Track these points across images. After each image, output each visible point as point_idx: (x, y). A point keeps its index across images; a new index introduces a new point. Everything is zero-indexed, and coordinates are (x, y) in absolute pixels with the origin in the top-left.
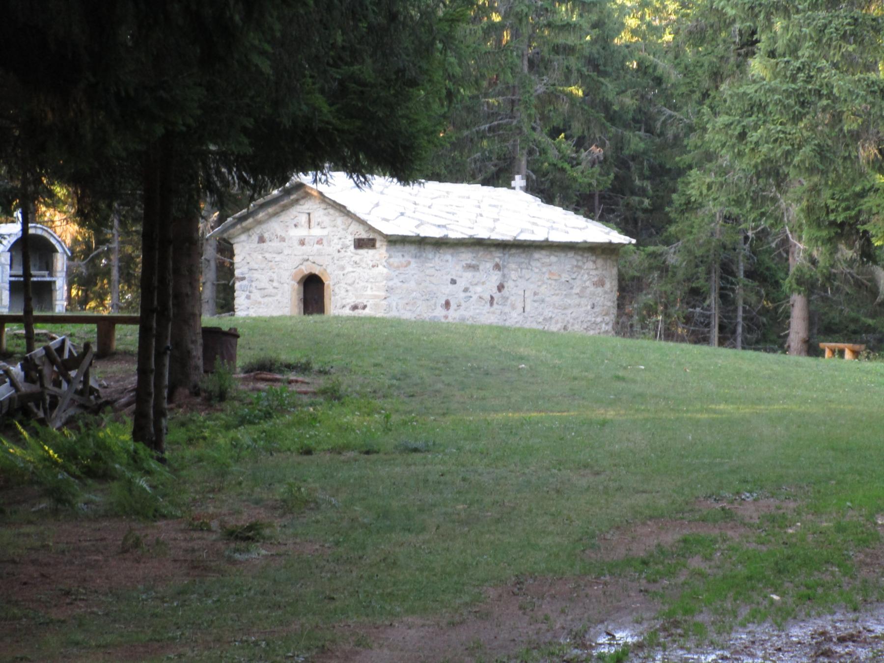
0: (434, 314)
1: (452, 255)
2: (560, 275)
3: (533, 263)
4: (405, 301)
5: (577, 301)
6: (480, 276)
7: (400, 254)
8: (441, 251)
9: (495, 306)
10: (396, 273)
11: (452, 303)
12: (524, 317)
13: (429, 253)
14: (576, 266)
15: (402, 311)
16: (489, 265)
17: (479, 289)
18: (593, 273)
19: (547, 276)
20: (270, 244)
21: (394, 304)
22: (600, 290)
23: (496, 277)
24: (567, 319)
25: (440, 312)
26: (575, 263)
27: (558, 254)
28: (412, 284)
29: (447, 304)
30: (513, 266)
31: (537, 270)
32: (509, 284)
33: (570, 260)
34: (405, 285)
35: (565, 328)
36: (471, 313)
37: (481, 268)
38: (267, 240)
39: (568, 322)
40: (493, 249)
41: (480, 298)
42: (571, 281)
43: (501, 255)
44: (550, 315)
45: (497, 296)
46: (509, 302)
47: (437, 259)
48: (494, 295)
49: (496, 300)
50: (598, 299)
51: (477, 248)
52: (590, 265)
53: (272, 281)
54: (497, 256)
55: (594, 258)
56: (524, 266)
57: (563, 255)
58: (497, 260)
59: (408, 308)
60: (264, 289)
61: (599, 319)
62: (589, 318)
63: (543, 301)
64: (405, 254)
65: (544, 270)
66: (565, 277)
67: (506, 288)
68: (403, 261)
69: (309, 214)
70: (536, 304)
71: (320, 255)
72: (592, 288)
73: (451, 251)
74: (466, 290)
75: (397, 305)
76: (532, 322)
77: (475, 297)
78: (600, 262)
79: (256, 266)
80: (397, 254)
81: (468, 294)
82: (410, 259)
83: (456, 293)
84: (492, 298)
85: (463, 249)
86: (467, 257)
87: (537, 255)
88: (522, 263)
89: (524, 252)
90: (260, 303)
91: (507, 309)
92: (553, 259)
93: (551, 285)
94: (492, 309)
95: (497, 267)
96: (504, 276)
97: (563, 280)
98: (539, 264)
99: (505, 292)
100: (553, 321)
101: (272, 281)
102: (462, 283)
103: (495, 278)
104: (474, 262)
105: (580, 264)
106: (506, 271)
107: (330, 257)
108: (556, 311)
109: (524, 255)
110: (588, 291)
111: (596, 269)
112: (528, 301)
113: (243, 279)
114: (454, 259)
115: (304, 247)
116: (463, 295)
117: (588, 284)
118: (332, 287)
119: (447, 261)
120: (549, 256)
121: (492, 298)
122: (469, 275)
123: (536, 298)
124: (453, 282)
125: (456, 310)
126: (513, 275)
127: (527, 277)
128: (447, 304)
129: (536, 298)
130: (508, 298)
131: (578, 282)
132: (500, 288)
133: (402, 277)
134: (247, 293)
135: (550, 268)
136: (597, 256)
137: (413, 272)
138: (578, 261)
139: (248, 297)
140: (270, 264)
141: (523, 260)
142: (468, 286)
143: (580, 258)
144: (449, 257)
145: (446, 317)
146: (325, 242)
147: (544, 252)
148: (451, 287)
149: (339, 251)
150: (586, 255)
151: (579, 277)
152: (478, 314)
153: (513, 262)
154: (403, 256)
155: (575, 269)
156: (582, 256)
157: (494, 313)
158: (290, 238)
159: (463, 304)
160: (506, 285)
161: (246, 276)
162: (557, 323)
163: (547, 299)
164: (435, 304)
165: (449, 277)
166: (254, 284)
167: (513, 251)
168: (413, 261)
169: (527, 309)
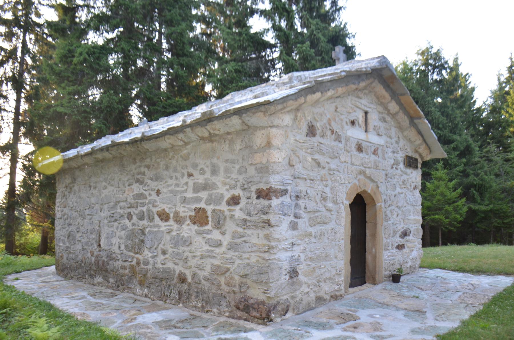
20: (321, 140)
38: (318, 132)
53: (325, 199)
60: (315, 212)
69: (366, 113)
71: (377, 167)
79: (304, 173)
90: (310, 235)
101: (325, 199)
107: (384, 172)
113: (285, 192)
115: (361, 155)
118: (384, 210)
134: (292, 218)
139: (294, 226)
140: (323, 172)
146: (379, 152)
149: (392, 168)
158: (347, 139)
161: (289, 188)
166: (301, 202)
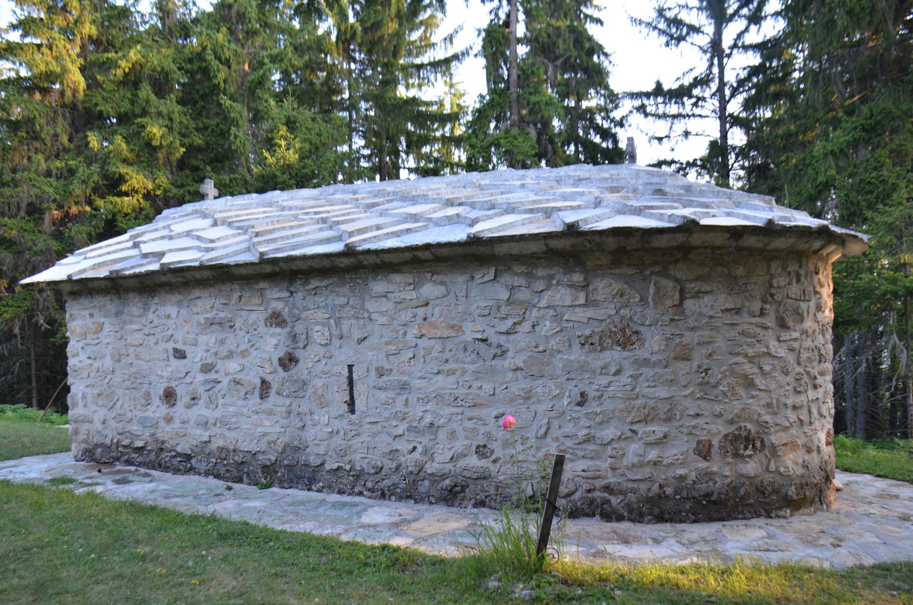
0: (147, 414)
1: (179, 304)
2: (458, 329)
3: (371, 306)
4: (96, 391)
5: (519, 386)
6: (236, 340)
7: (86, 313)
8: (156, 300)
9: (273, 397)
10: (81, 344)
11: (181, 391)
12: (351, 423)
13: (134, 305)
14: (509, 302)
15: (94, 408)
16: (258, 316)
17: (233, 366)
18: (582, 314)
19: (414, 331)
21: (80, 396)
22: (614, 356)
23: (274, 341)
24: (482, 430)
25: (157, 410)
26: (504, 295)
27: (447, 279)
28: (108, 362)
29: (169, 396)
30: (321, 315)
31: (383, 320)
32: (307, 359)
33: (484, 292)
34: (97, 364)
35: (482, 451)
36: (217, 414)
37: (239, 323)
39: (488, 435)
40: (263, 285)
41: (237, 383)
42: (494, 339)
43: (286, 294)
44: (428, 419)
45: (277, 378)
46: (310, 391)
47: (151, 316)
48: (269, 378)
49: (275, 387)
50: (604, 380)
51: (226, 287)
52: (561, 296)
54: (276, 298)
55: (578, 278)
56: (348, 312)
57: (461, 279)
58: (279, 306)
59: (101, 403)
61: (609, 433)
62: (569, 428)
63: (404, 387)
64: (96, 312)
65: (405, 316)
66: (470, 331)
67: (300, 364)
68: (89, 321)
70: (382, 395)
72: (577, 354)
73: (177, 297)
74: (207, 368)
75: (84, 397)
76: (375, 435)
77: (225, 381)
78: (604, 287)
80: (82, 312)
81: (212, 376)
82: (102, 320)
83: (188, 375)
84: (263, 382)
85: (197, 292)
86: (207, 305)
87: (378, 286)
88: (342, 306)
89: (344, 284)
91: (304, 408)
92: (430, 290)
93: (428, 351)
94: (268, 404)
95: (276, 319)
96: (294, 337)
97: (469, 336)
98: (387, 306)
99: (301, 370)
100: (442, 435)
102: (196, 356)
103: (273, 343)
104: (222, 315)
105: (523, 295)
106: (299, 328)
108: (448, 410)
109: (346, 290)
110: (559, 362)
111: (588, 304)
112: (358, 388)
114: (184, 312)
116: (201, 377)
117: (553, 343)
119: (168, 317)
120: (416, 286)
121: (263, 382)
122: (209, 339)
123: (381, 382)
124: (180, 355)
125: (188, 407)
126: (319, 335)
127: (357, 335)
128: (169, 396)
129: (381, 382)
130: (304, 383)
131: (521, 338)
132: (288, 361)
133: (89, 349)
135: (421, 312)
136: (589, 274)
137: (108, 340)
138: (512, 289)
141: (343, 300)
142: (209, 361)
143: (519, 281)
144: (172, 310)
145: (169, 420)
147: (397, 278)
148: (175, 363)
150: (540, 272)
151: (526, 326)
152: (236, 415)
153: (316, 308)
154: (91, 315)
155: (504, 310)
156: (529, 275)
157: (270, 413)
159: (204, 397)
160: (299, 354)
162: (453, 435)
163: (416, 383)
164: (148, 395)
165: (171, 345)
167: (315, 283)
168: (107, 321)
169: (359, 405)
